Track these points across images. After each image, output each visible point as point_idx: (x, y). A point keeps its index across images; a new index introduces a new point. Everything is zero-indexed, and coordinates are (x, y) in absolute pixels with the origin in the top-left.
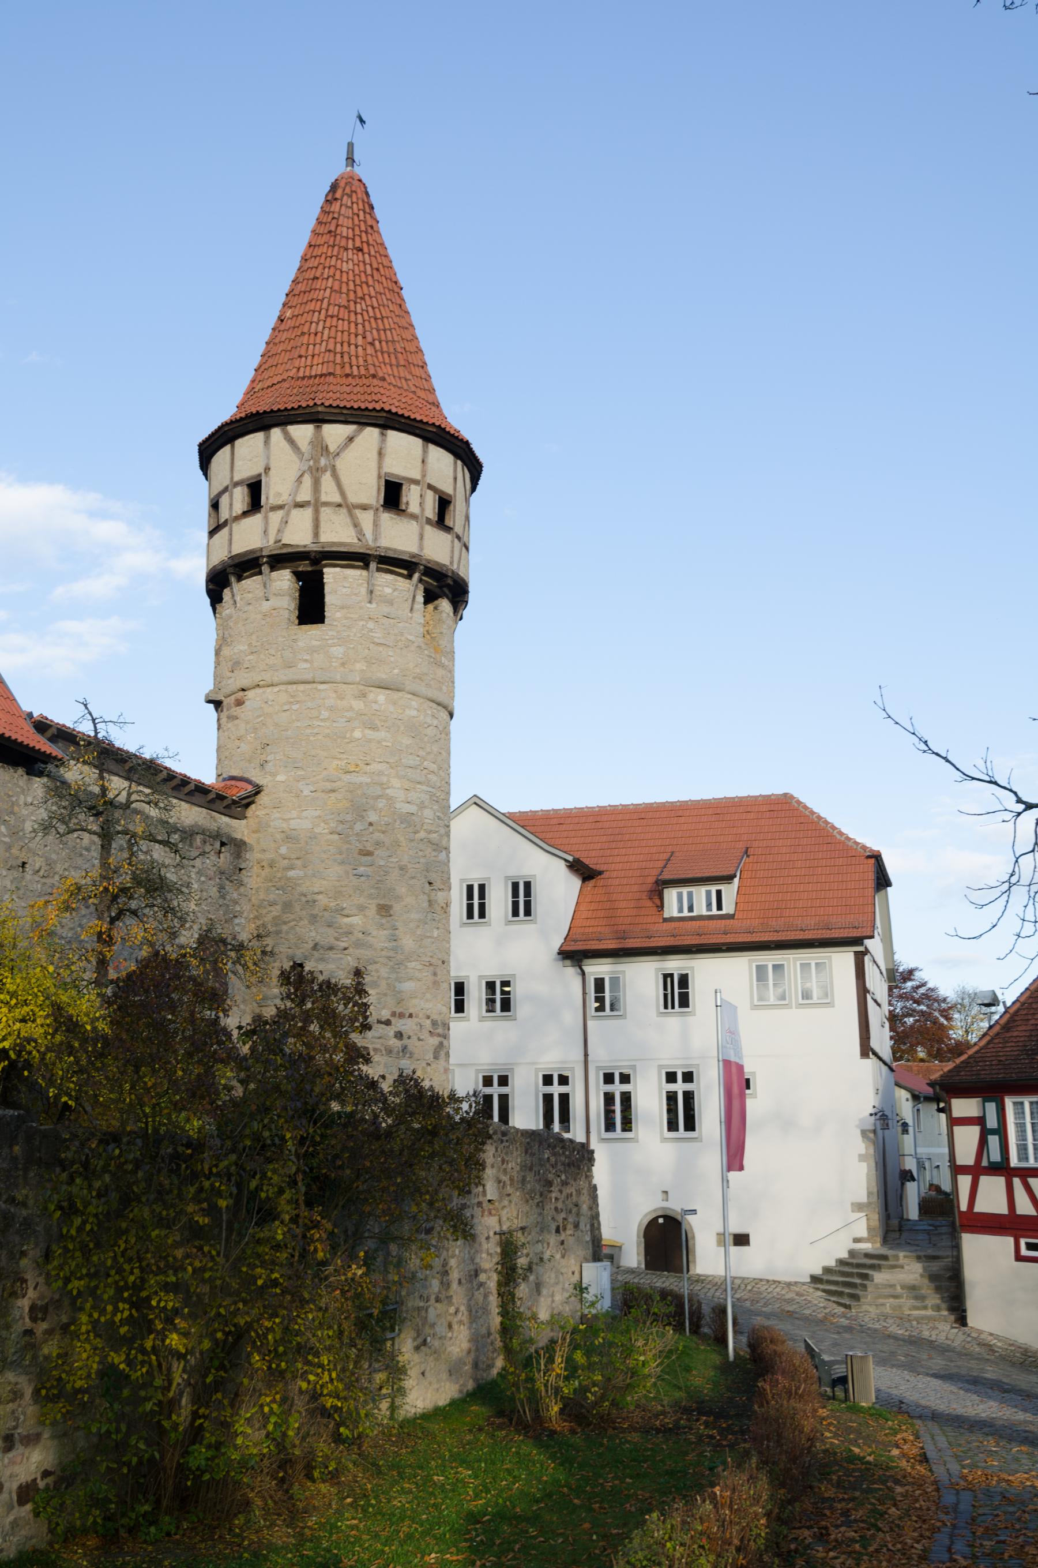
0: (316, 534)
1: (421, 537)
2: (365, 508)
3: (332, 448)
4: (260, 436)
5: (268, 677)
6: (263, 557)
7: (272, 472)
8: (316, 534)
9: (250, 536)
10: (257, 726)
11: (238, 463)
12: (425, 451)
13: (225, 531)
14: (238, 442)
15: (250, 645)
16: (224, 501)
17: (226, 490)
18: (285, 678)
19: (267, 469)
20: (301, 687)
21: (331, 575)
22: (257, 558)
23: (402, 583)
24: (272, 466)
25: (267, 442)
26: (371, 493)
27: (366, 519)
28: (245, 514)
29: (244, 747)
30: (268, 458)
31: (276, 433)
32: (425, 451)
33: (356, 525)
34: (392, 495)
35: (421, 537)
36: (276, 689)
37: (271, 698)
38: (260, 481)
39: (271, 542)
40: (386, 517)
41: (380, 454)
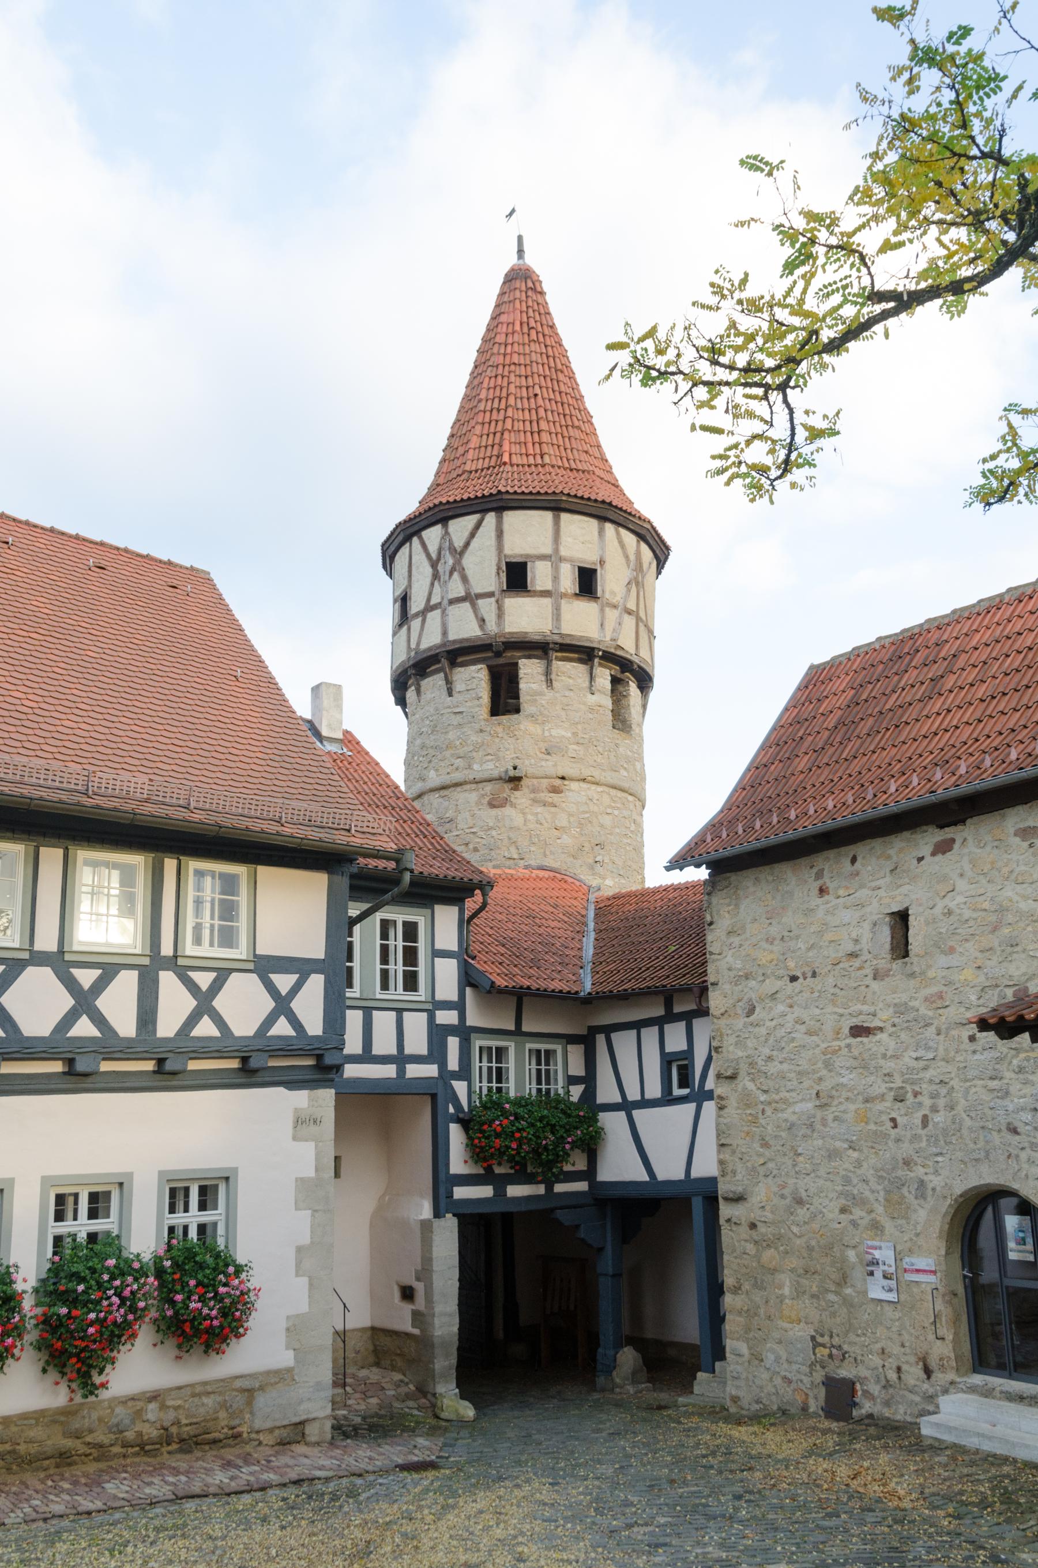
5: (597, 774)
6: (599, 650)
7: (607, 566)
10: (583, 821)
11: (566, 539)
13: (547, 602)
15: (575, 734)
18: (611, 781)
20: (620, 794)
22: (593, 649)
24: (608, 559)
25: (601, 532)
29: (566, 840)
30: (603, 548)
31: (609, 527)
36: (600, 789)
37: (596, 797)
38: (595, 570)
39: (608, 639)
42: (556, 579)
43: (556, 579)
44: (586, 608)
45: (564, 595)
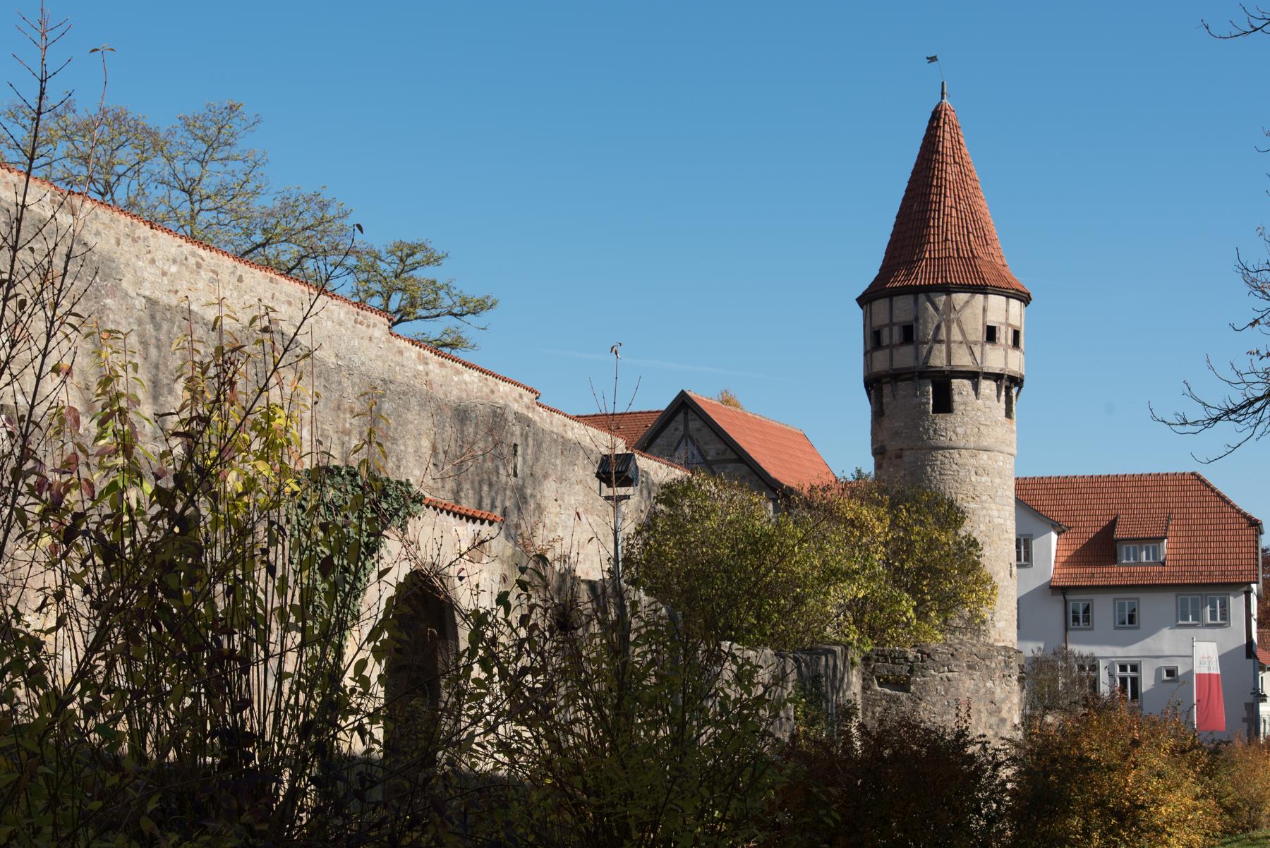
0: (949, 360)
1: (1006, 358)
2: (975, 343)
3: (958, 308)
4: (910, 298)
8: (949, 360)
9: (905, 358)
12: (1008, 303)
13: (887, 351)
14: (895, 299)
16: (885, 334)
17: (885, 326)
19: (917, 319)
21: (956, 383)
23: (993, 385)
26: (979, 334)
27: (977, 350)
28: (902, 344)
30: (917, 311)
31: (922, 297)
32: (1008, 303)
33: (972, 353)
34: (991, 334)
35: (1006, 358)
40: (988, 347)
41: (985, 310)
42: (891, 337)
43: (891, 337)
44: (909, 349)
45: (895, 345)
